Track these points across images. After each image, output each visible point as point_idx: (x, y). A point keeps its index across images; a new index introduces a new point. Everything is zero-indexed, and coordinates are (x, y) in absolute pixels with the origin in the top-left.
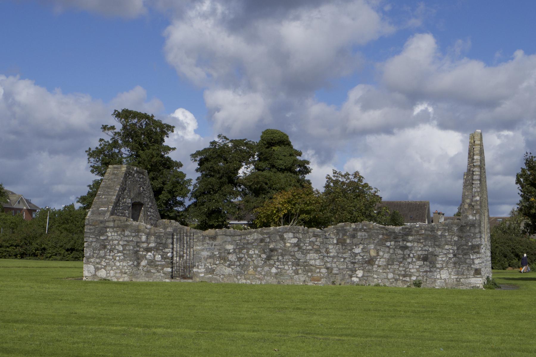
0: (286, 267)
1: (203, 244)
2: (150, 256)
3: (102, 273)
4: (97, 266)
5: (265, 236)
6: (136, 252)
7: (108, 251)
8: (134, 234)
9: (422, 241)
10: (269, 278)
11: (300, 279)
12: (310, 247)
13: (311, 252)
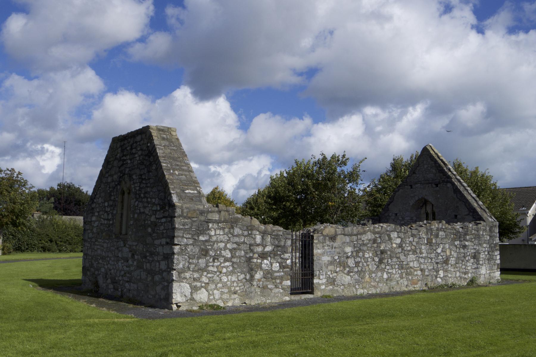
0: (394, 272)
1: (323, 247)
2: (267, 264)
3: (202, 296)
4: (195, 283)
5: (377, 236)
6: (249, 260)
7: (211, 260)
8: (246, 233)
9: (473, 240)
10: (382, 285)
11: (403, 285)
12: (409, 248)
13: (411, 253)
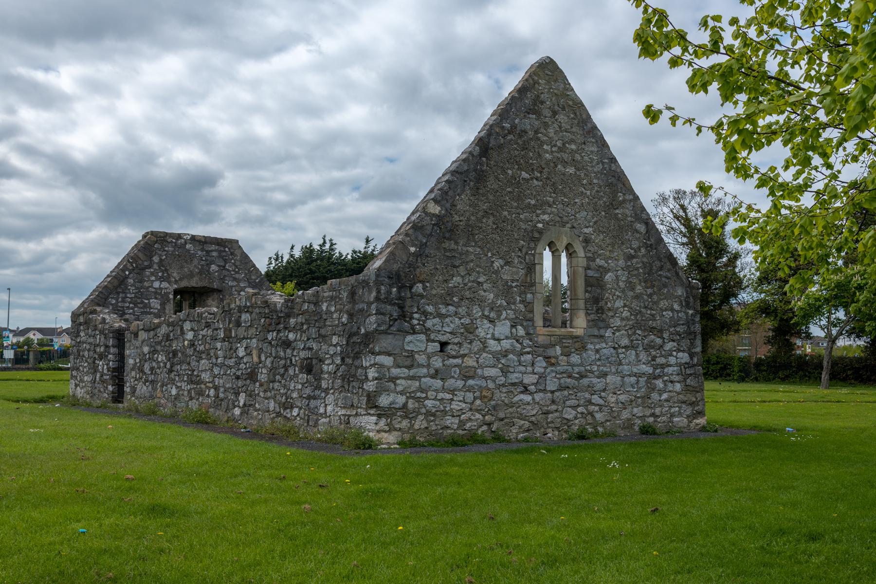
9: (305, 327)
